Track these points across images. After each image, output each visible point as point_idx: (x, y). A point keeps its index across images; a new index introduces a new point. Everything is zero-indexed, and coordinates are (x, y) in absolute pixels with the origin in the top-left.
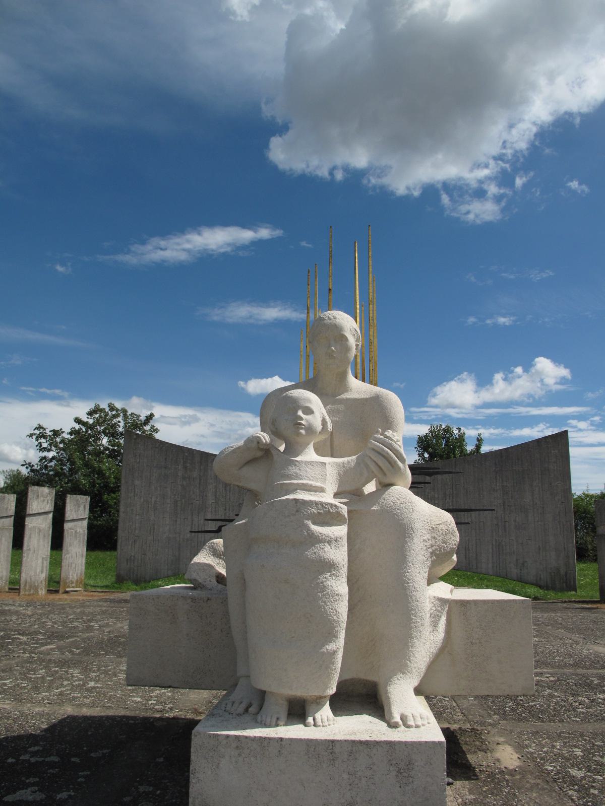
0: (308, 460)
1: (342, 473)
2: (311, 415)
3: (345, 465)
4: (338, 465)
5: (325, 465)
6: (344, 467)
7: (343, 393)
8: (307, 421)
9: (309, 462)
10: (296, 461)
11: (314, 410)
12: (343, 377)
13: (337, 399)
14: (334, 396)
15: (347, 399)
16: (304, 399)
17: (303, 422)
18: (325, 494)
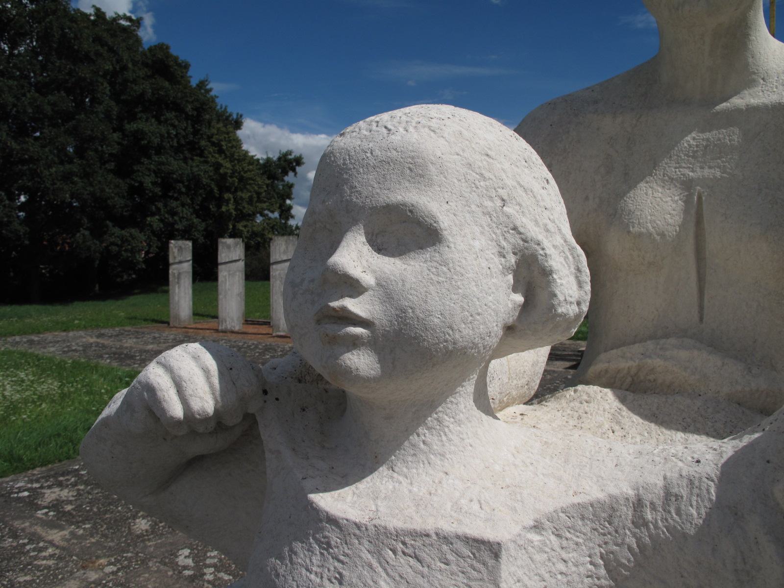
0: (394, 523)
1: (625, 557)
2: (429, 253)
3: (649, 516)
4: (602, 515)
5: (497, 556)
6: (639, 522)
7: (736, 92)
8: (387, 291)
9: (398, 535)
10: (333, 521)
11: (445, 221)
12: (736, 39)
13: (718, 113)
14: (710, 102)
15: (752, 110)
16: (388, 162)
17: (354, 305)
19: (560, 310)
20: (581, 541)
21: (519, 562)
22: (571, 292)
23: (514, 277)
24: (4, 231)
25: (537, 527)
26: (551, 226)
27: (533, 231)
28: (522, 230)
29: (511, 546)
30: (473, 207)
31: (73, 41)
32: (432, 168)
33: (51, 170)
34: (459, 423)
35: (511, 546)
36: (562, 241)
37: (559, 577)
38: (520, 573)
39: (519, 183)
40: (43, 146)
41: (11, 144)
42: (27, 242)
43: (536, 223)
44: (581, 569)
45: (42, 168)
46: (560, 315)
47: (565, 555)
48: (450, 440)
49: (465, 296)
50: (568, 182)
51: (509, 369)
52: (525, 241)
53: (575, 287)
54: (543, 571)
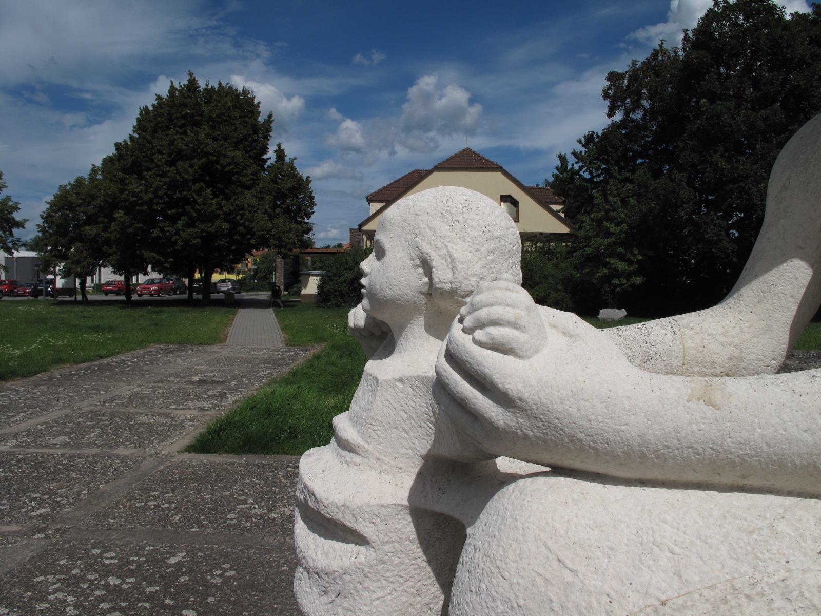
18: (358, 459)
19: (437, 286)
20: (422, 395)
21: (389, 392)
22: (445, 277)
23: (424, 269)
24: (713, 250)
25: (401, 380)
26: (439, 245)
27: (426, 247)
28: (420, 248)
29: (385, 384)
30: (402, 239)
31: (785, 50)
32: (387, 223)
33: (759, 186)
34: (415, 338)
35: (385, 384)
36: (446, 252)
37: (411, 408)
38: (389, 397)
39: (428, 226)
40: (754, 163)
41: (721, 164)
42: (735, 260)
43: (430, 244)
44: (422, 409)
45: (750, 186)
46: (439, 288)
47: (414, 399)
48: (410, 345)
49: (387, 277)
50: (807, 192)
51: (684, 356)
52: (422, 253)
53: (451, 274)
54: (402, 402)
